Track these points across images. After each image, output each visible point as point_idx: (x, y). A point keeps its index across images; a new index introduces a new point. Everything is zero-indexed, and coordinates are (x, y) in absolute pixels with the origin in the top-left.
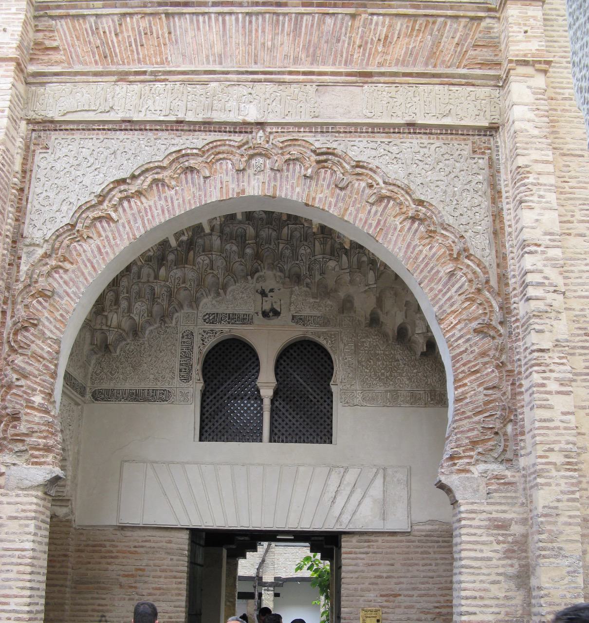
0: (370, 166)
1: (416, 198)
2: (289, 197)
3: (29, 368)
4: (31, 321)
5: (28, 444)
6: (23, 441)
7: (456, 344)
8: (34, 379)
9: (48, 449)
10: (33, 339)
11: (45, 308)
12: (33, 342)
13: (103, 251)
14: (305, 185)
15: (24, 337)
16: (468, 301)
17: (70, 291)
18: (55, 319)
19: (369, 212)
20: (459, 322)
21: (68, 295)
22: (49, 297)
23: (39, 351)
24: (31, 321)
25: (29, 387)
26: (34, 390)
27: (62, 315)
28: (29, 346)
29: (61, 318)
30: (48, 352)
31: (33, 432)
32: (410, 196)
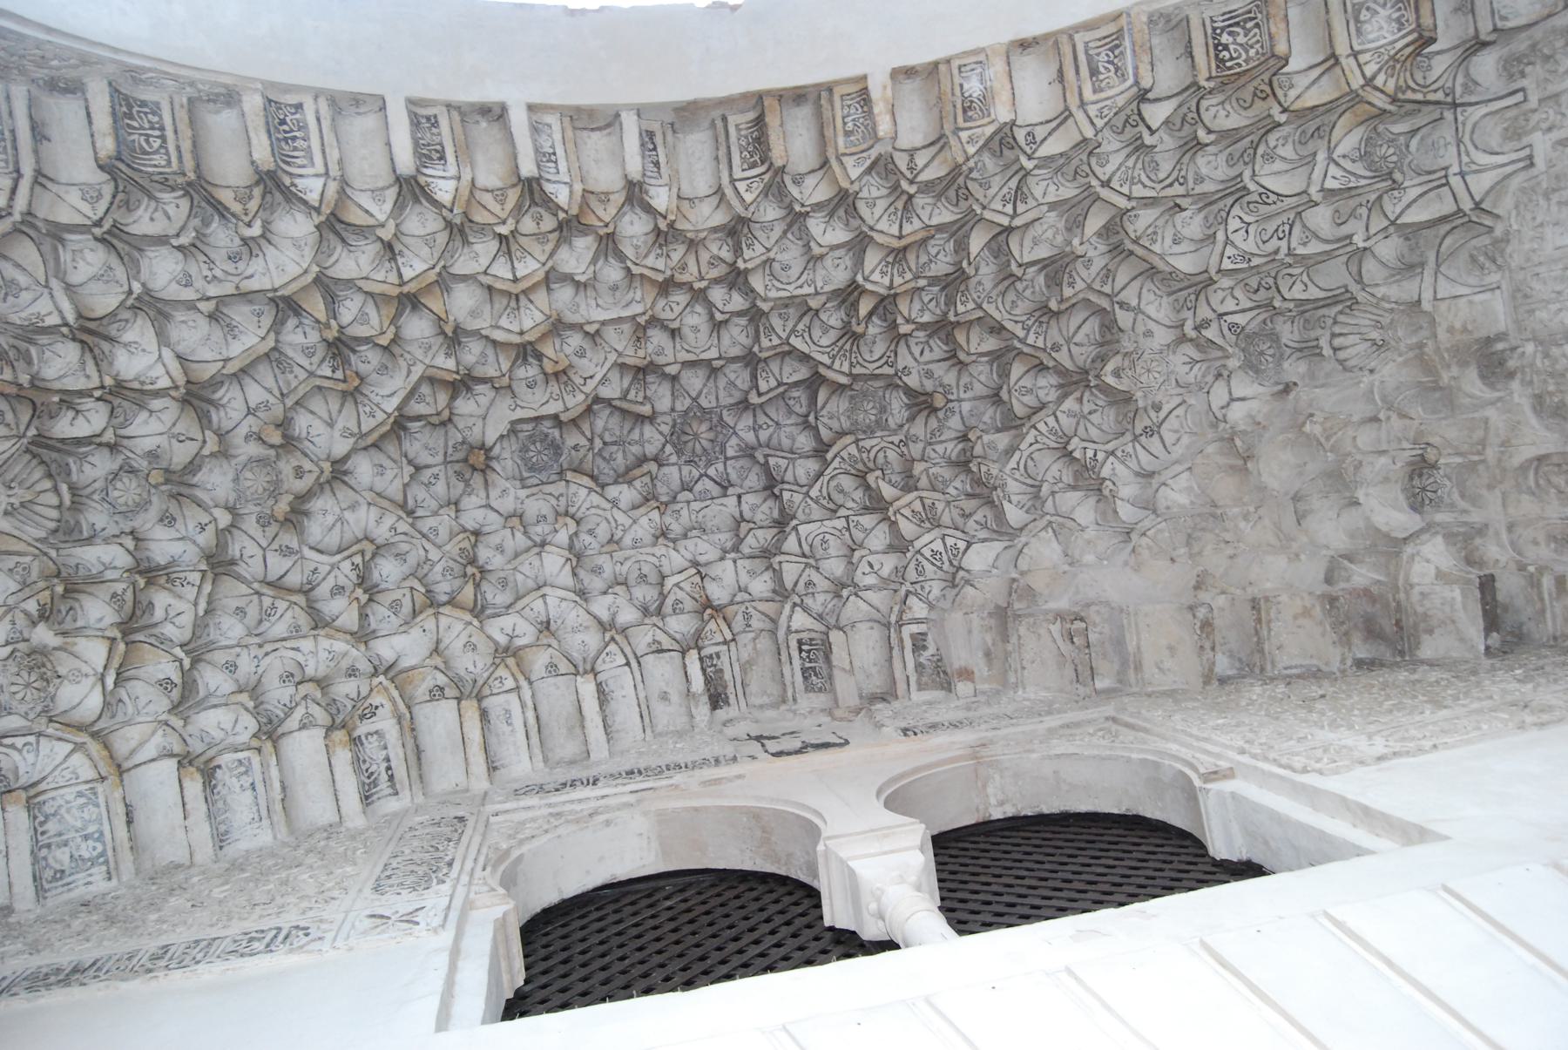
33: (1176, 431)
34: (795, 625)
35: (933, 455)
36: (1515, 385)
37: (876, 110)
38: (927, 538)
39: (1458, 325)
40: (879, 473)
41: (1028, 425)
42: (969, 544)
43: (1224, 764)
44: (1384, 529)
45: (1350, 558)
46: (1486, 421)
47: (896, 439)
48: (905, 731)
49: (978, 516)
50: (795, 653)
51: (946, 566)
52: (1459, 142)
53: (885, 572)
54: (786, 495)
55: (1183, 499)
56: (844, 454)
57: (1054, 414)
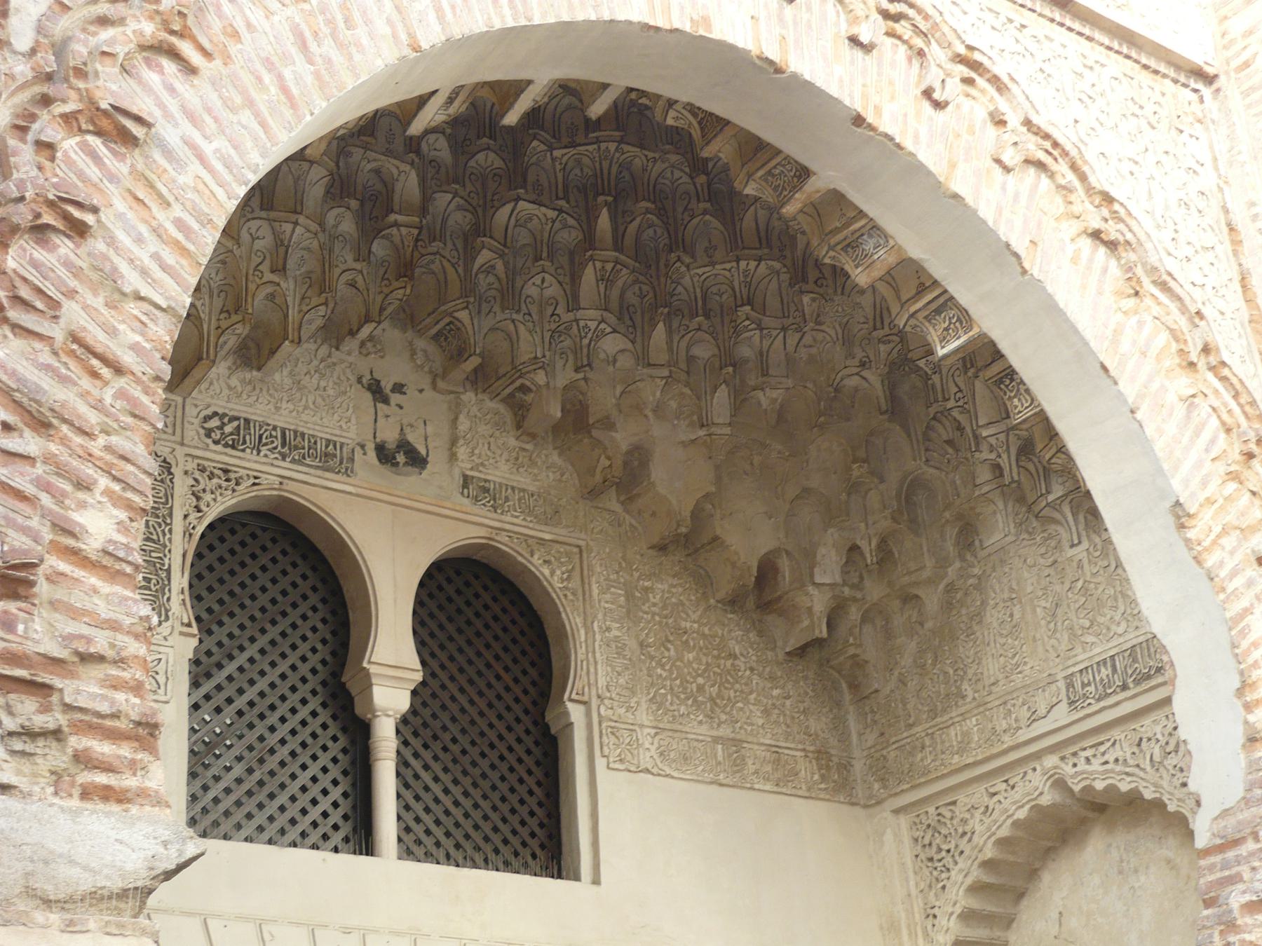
0: (996, 70)
1: (1098, 187)
2: (819, 83)
3: (56, 393)
4: (76, 213)
5: (68, 708)
6: (44, 689)
7: (1230, 589)
8: (78, 440)
9: (146, 732)
10: (73, 283)
11: (113, 178)
12: (71, 294)
13: (313, 46)
14: (852, 62)
15: (35, 265)
16: (1233, 479)
17: (208, 148)
18: (157, 232)
19: (1004, 189)
20: (1225, 531)
21: (201, 158)
22: (129, 140)
23: (97, 337)
24: (71, 209)
25: (61, 471)
26: (83, 485)
27: (179, 223)
28: (54, 304)
29: (180, 237)
30: (135, 347)
31: (85, 658)
32: (1083, 178)
33: (815, 340)
34: (456, 314)
35: (669, 175)
36: (958, 564)
37: (797, 196)
38: (592, 313)
39: (978, 510)
40: (610, 199)
41: (738, 253)
42: (615, 331)
43: (586, 698)
44: (819, 557)
45: (788, 553)
46: (922, 568)
47: (651, 155)
48: (466, 481)
49: (645, 288)
50: (442, 324)
51: (585, 341)
52: (1066, 495)
53: (548, 292)
54: (535, 143)
55: (765, 403)
56: (603, 146)
57: (760, 260)
